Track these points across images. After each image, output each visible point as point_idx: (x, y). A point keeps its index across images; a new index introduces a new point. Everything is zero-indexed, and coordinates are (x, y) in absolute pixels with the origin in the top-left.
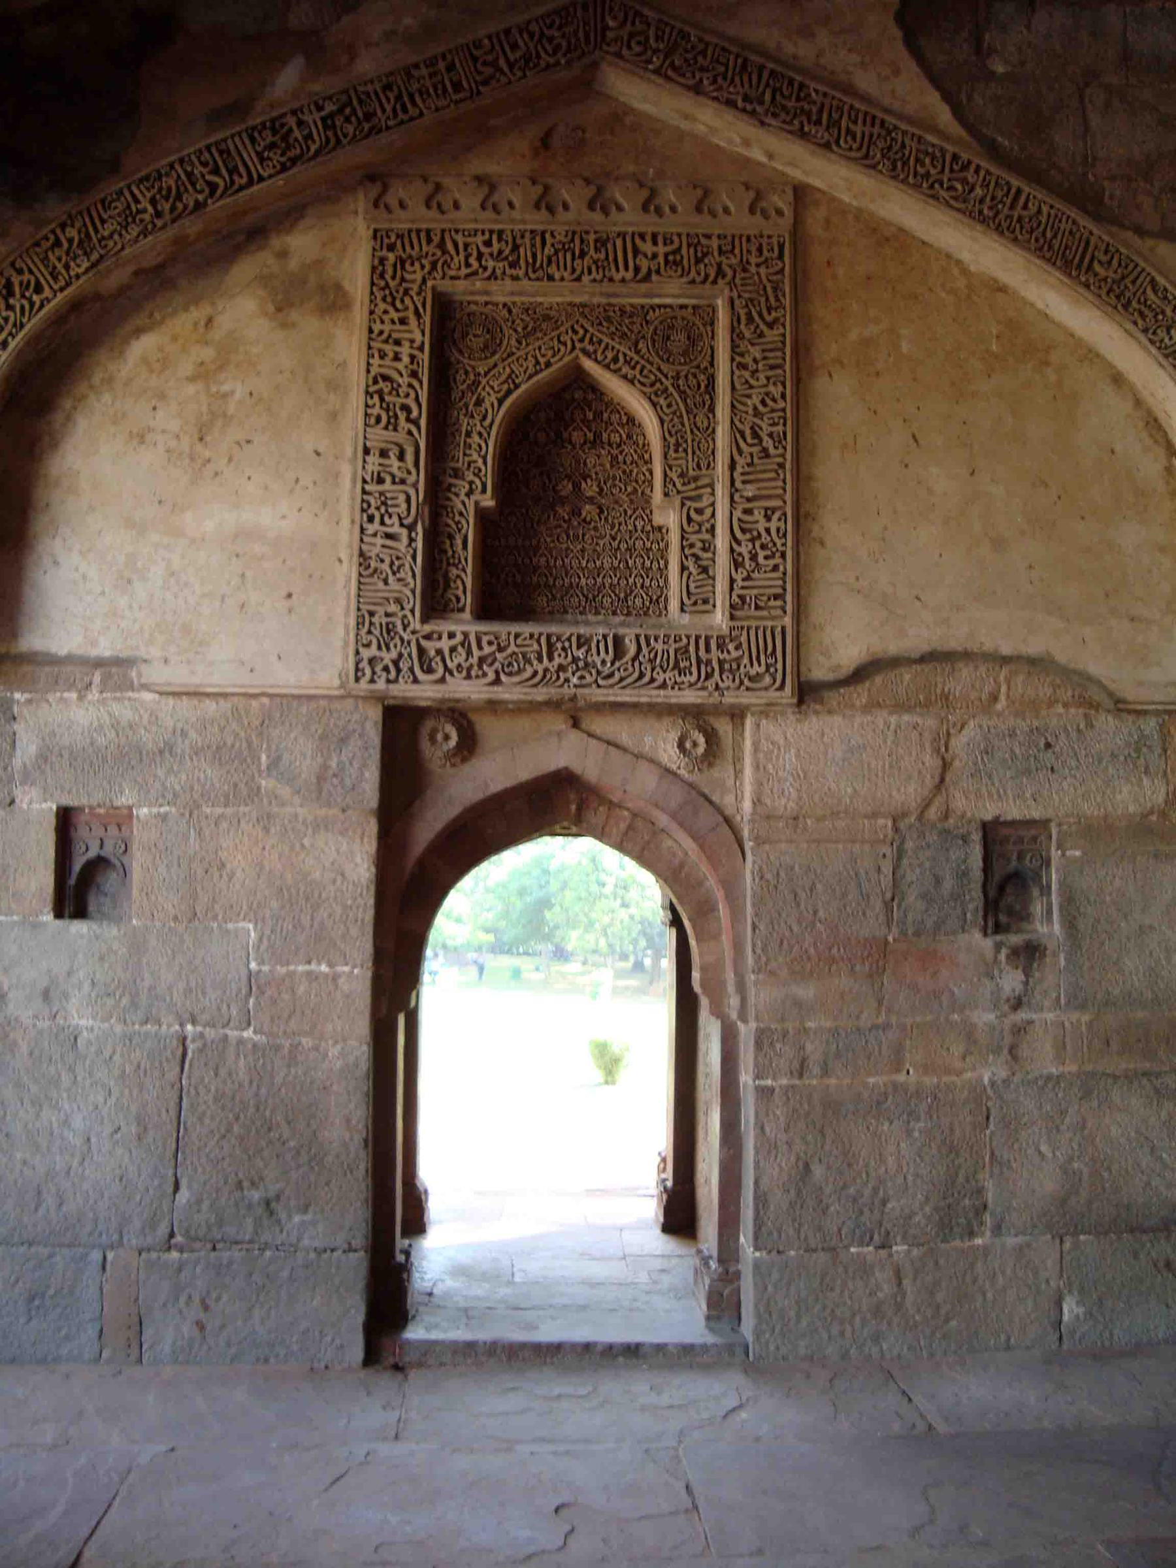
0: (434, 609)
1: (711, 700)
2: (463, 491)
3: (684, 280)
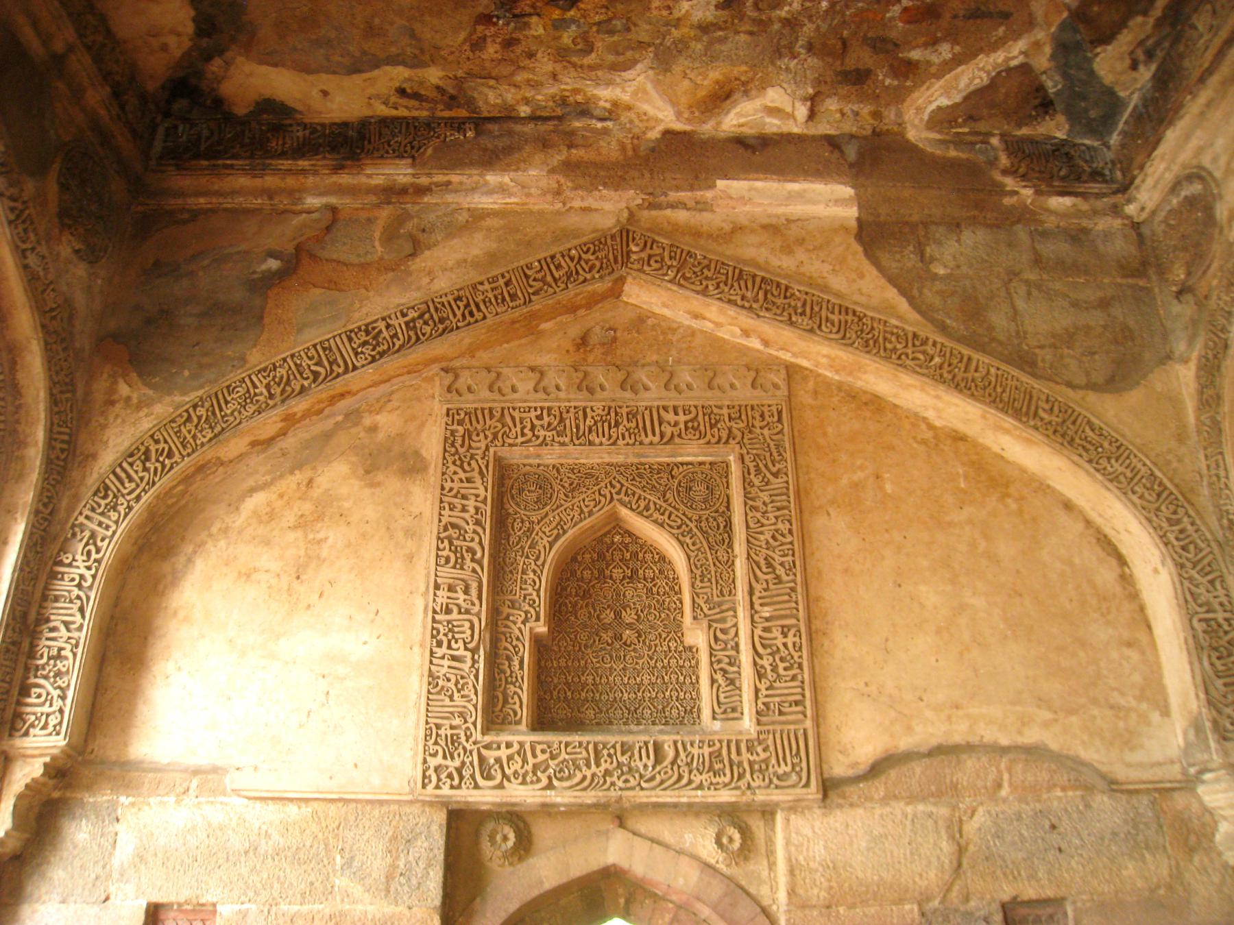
0: (493, 722)
1: (744, 799)
2: (520, 619)
3: (702, 441)
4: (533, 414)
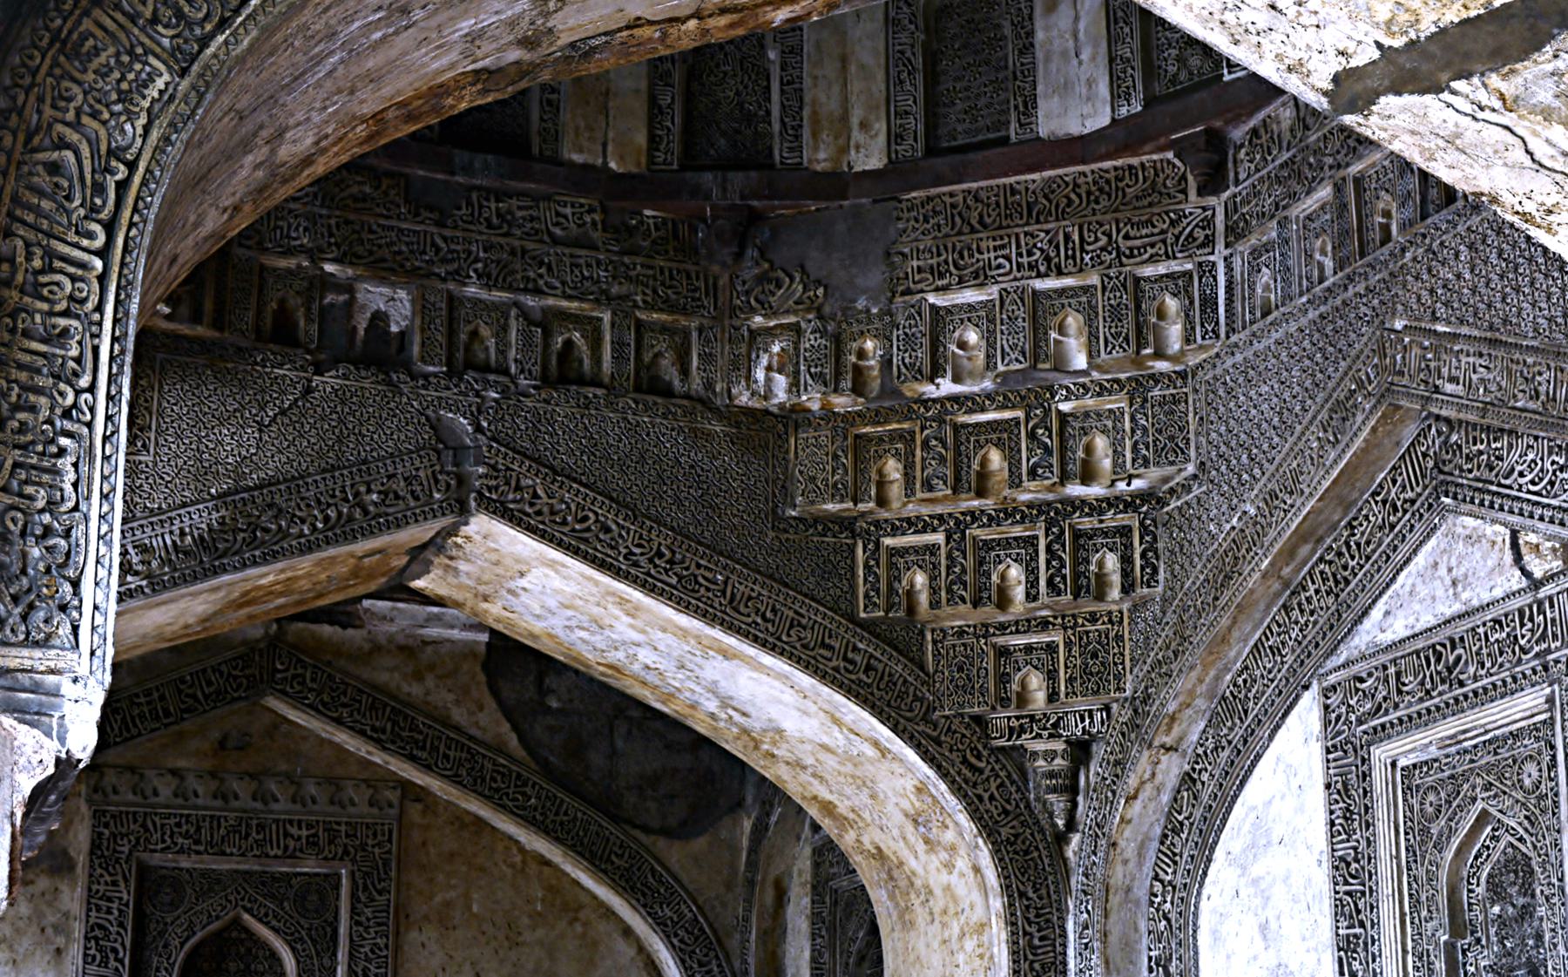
4: (172, 821)
